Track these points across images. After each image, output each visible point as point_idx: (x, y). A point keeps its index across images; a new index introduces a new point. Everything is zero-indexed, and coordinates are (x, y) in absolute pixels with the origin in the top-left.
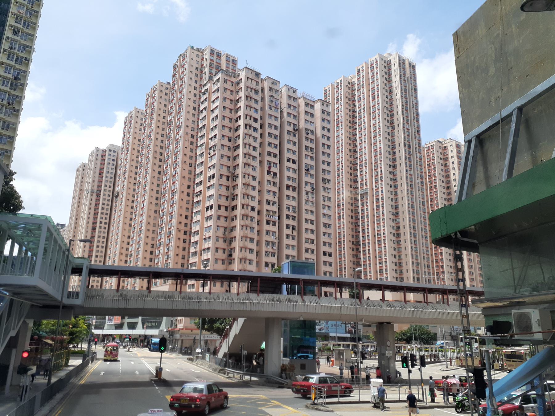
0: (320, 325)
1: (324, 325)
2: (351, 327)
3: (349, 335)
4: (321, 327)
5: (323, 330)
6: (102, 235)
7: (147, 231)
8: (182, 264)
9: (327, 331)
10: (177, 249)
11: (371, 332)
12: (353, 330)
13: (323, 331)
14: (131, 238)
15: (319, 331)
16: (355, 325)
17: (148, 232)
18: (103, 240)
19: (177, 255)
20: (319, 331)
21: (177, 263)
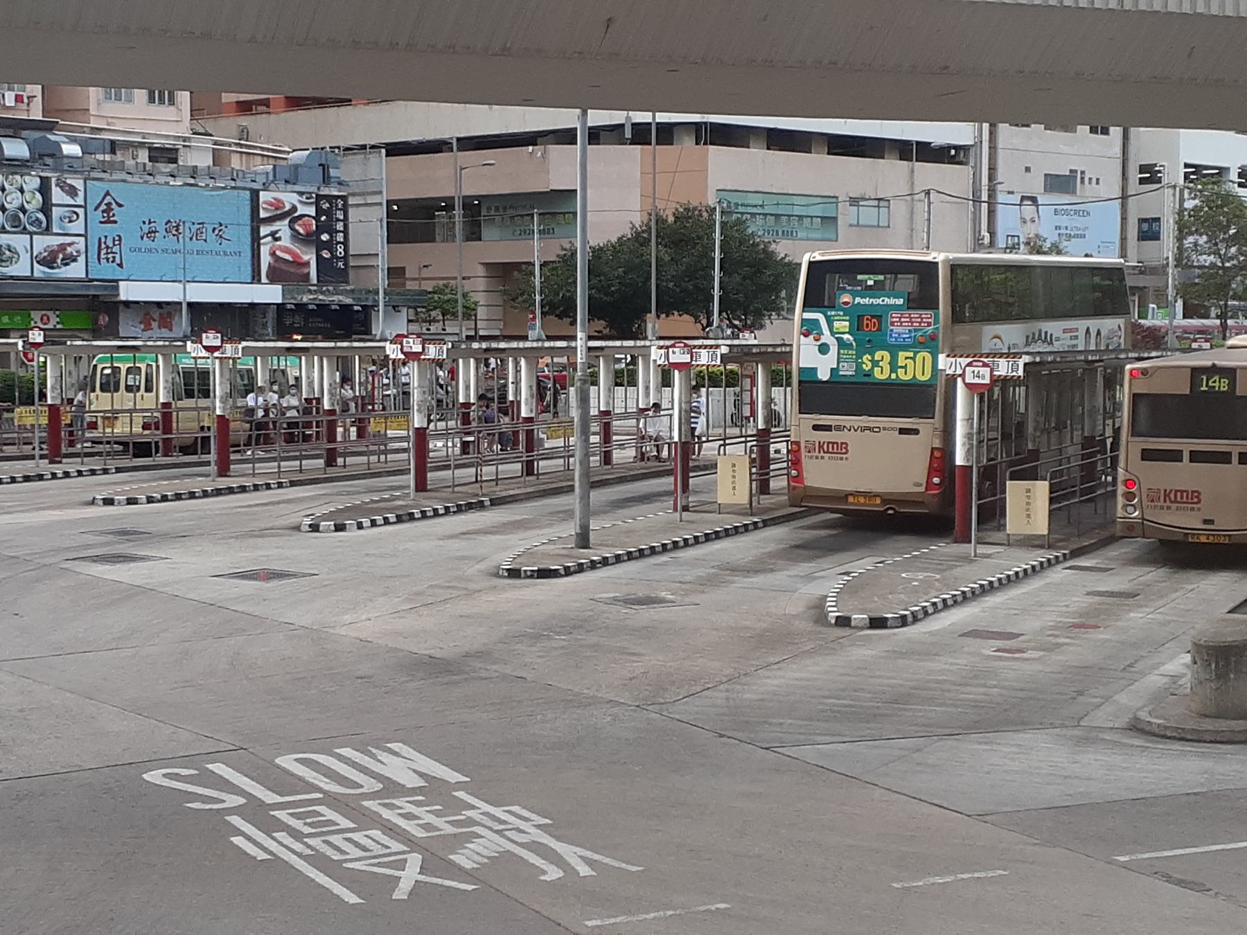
0: (48, 231)
1: (78, 227)
2: (296, 236)
3: (271, 294)
4: (54, 241)
5: (70, 259)
9: (105, 271)
11: (481, 271)
12: (310, 257)
13: (75, 271)
15: (40, 271)
16: (321, 229)
20: (40, 271)
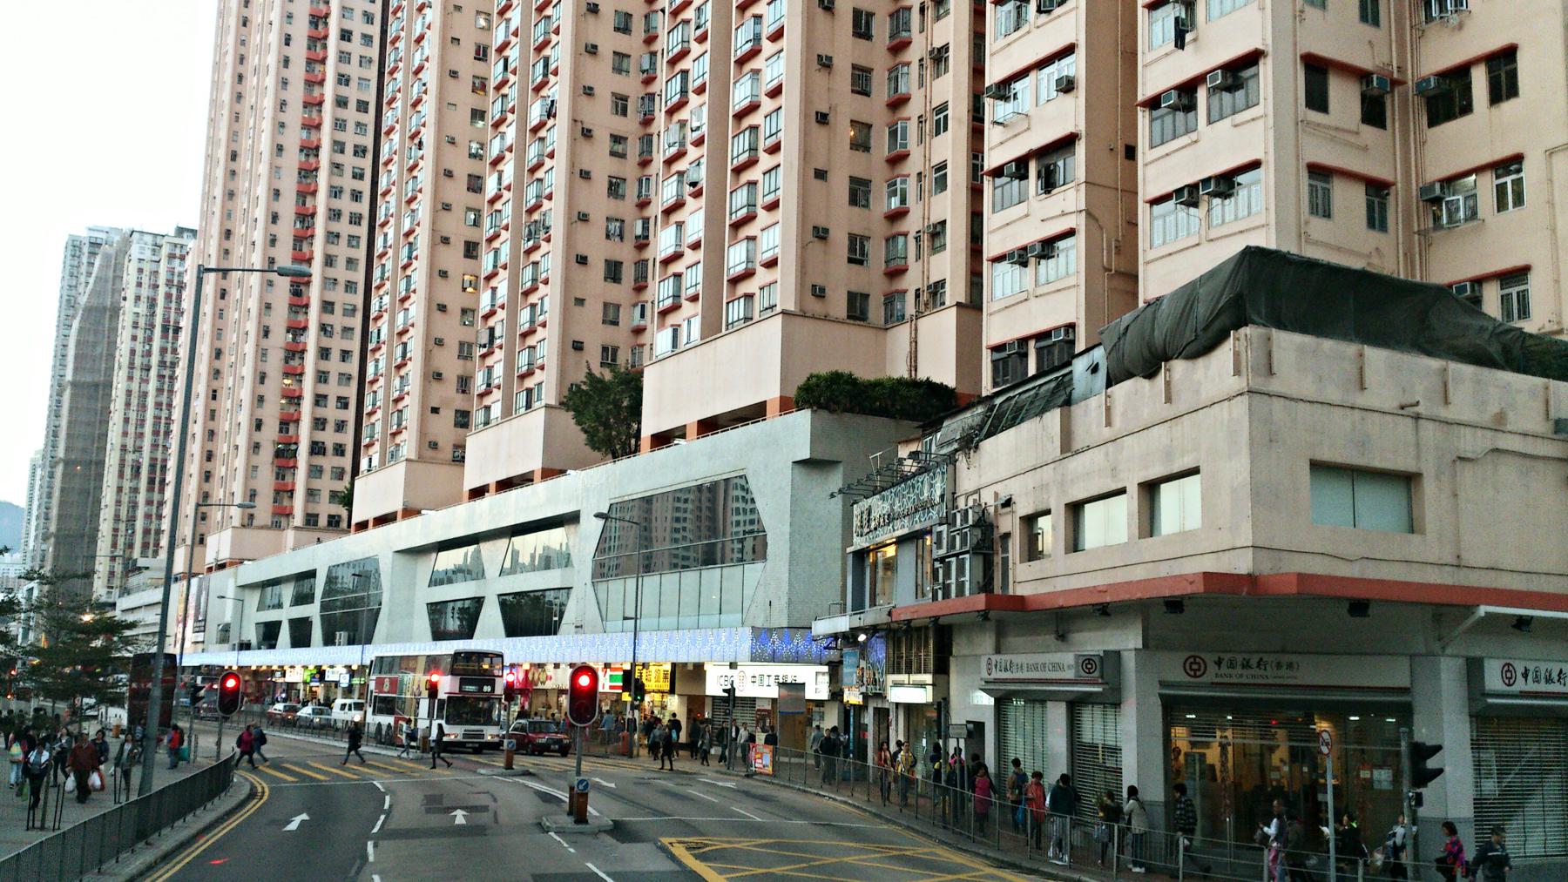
6: (348, 183)
7: (587, 58)
10: (820, 78)
14: (492, 83)
17: (587, 60)
18: (354, 230)
21: (821, 175)
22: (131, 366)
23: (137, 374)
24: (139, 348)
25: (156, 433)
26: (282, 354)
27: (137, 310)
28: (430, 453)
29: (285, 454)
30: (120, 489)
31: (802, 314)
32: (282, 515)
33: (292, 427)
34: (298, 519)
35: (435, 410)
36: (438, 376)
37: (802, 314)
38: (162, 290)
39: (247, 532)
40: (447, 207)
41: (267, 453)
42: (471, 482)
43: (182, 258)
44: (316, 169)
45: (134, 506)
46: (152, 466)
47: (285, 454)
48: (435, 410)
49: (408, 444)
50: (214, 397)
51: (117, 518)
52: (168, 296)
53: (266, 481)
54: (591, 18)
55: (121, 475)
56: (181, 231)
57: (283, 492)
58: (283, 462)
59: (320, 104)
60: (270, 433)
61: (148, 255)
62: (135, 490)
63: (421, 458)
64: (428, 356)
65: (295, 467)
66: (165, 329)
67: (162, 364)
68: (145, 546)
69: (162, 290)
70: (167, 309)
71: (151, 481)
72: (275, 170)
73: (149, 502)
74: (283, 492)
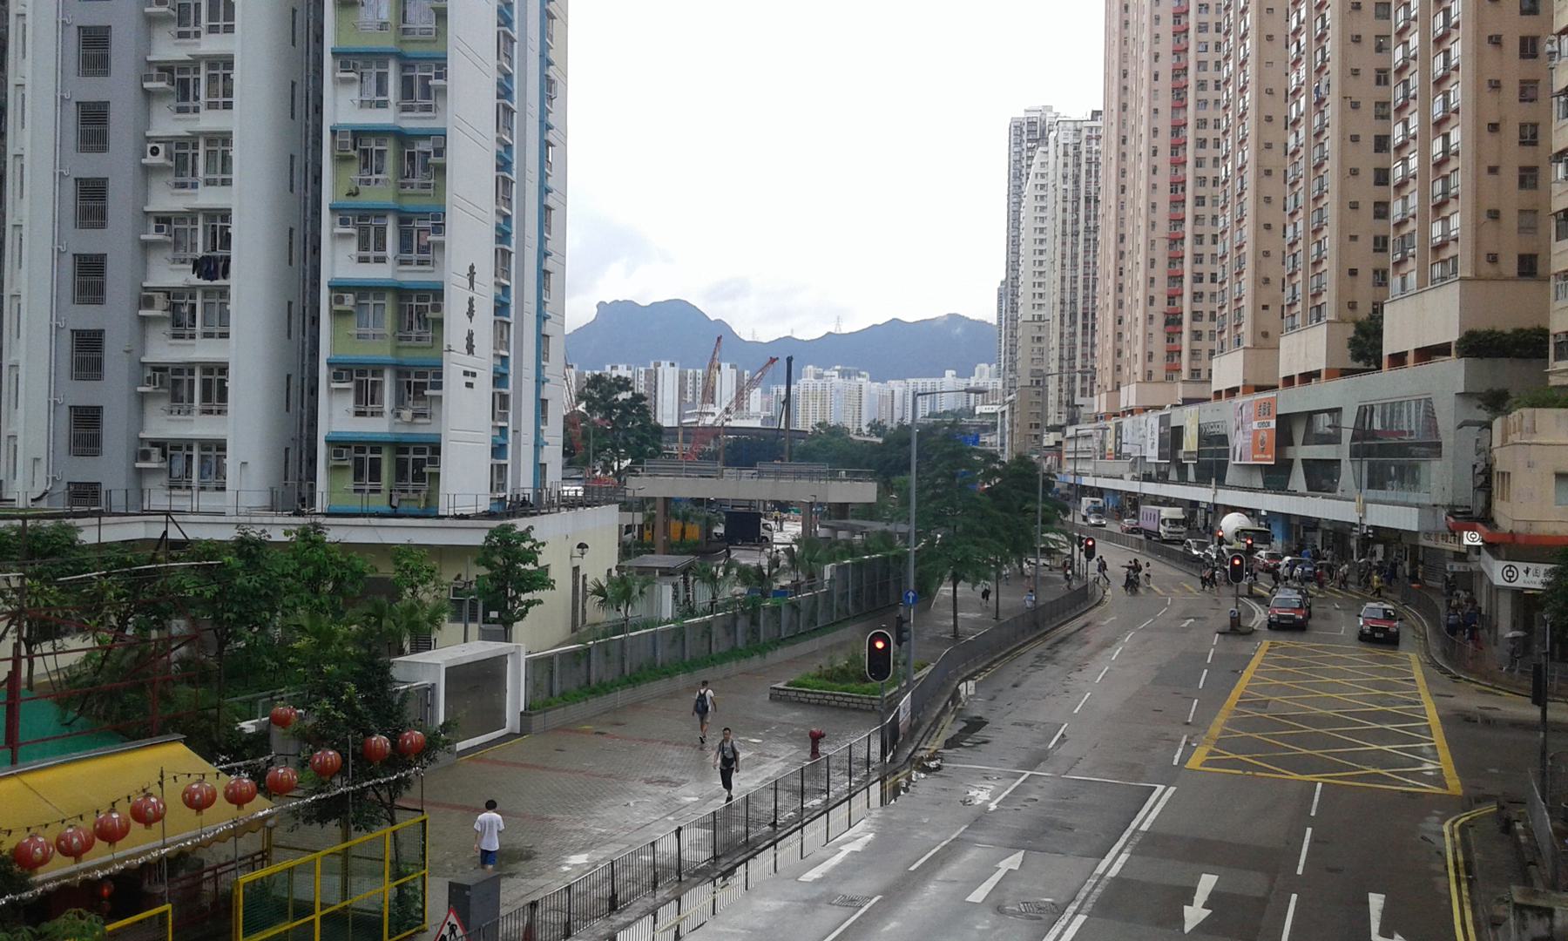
8: (1522, 169)
19: (1494, 127)
21: (1493, 170)
22: (1064, 234)
23: (1069, 239)
24: (1069, 218)
25: (1086, 287)
26: (1167, 242)
27: (1065, 187)
28: (1262, 341)
29: (1173, 321)
30: (1062, 335)
31: (1477, 278)
32: (1173, 370)
33: (1177, 300)
34: (1185, 375)
35: (1265, 307)
36: (1267, 281)
37: (1477, 278)
38: (1084, 167)
39: (1148, 386)
40: (1269, 146)
41: (1159, 321)
42: (1283, 373)
43: (1098, 138)
44: (1186, 87)
45: (1073, 348)
46: (1085, 315)
47: (1173, 321)
48: (1265, 307)
49: (1246, 329)
50: (1121, 274)
51: (1061, 358)
52: (1088, 172)
53: (1159, 345)
54: (1355, 14)
55: (1062, 323)
56: (1096, 114)
57: (1173, 353)
58: (1171, 328)
59: (1187, 31)
60: (1161, 305)
61: (1071, 140)
62: (1074, 334)
63: (1255, 346)
64: (1257, 264)
65: (1181, 333)
66: (1088, 200)
67: (1087, 229)
68: (1083, 391)
69: (1084, 167)
70: (1088, 183)
71: (1085, 327)
72: (1154, 93)
73: (1084, 344)
74: (1173, 353)
